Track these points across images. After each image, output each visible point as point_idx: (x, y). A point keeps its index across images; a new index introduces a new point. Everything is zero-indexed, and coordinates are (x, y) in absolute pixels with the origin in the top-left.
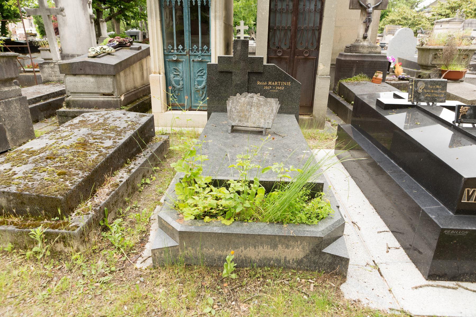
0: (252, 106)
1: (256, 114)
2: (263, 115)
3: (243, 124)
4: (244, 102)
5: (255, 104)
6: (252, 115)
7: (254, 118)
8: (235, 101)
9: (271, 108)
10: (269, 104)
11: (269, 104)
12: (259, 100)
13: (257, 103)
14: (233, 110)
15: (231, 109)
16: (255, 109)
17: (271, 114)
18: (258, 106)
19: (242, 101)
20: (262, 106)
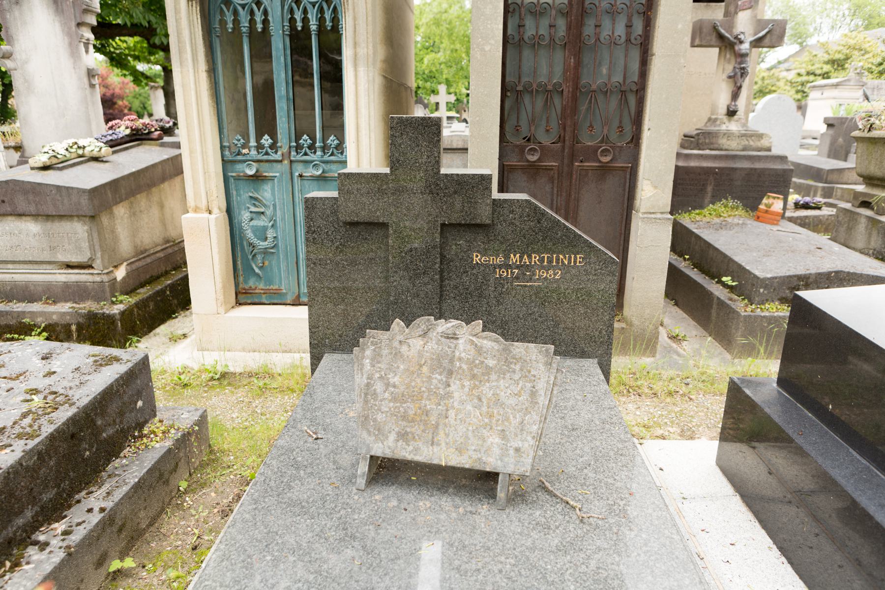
0: (450, 373)
1: (469, 407)
2: (497, 417)
3: (417, 450)
4: (420, 354)
5: (465, 367)
6: (452, 413)
7: (462, 429)
8: (385, 352)
9: (529, 385)
10: (518, 367)
11: (518, 367)
12: (479, 350)
13: (471, 363)
14: (379, 387)
15: (368, 385)
16: (463, 386)
17: (527, 412)
18: (474, 377)
19: (413, 352)
20: (493, 377)
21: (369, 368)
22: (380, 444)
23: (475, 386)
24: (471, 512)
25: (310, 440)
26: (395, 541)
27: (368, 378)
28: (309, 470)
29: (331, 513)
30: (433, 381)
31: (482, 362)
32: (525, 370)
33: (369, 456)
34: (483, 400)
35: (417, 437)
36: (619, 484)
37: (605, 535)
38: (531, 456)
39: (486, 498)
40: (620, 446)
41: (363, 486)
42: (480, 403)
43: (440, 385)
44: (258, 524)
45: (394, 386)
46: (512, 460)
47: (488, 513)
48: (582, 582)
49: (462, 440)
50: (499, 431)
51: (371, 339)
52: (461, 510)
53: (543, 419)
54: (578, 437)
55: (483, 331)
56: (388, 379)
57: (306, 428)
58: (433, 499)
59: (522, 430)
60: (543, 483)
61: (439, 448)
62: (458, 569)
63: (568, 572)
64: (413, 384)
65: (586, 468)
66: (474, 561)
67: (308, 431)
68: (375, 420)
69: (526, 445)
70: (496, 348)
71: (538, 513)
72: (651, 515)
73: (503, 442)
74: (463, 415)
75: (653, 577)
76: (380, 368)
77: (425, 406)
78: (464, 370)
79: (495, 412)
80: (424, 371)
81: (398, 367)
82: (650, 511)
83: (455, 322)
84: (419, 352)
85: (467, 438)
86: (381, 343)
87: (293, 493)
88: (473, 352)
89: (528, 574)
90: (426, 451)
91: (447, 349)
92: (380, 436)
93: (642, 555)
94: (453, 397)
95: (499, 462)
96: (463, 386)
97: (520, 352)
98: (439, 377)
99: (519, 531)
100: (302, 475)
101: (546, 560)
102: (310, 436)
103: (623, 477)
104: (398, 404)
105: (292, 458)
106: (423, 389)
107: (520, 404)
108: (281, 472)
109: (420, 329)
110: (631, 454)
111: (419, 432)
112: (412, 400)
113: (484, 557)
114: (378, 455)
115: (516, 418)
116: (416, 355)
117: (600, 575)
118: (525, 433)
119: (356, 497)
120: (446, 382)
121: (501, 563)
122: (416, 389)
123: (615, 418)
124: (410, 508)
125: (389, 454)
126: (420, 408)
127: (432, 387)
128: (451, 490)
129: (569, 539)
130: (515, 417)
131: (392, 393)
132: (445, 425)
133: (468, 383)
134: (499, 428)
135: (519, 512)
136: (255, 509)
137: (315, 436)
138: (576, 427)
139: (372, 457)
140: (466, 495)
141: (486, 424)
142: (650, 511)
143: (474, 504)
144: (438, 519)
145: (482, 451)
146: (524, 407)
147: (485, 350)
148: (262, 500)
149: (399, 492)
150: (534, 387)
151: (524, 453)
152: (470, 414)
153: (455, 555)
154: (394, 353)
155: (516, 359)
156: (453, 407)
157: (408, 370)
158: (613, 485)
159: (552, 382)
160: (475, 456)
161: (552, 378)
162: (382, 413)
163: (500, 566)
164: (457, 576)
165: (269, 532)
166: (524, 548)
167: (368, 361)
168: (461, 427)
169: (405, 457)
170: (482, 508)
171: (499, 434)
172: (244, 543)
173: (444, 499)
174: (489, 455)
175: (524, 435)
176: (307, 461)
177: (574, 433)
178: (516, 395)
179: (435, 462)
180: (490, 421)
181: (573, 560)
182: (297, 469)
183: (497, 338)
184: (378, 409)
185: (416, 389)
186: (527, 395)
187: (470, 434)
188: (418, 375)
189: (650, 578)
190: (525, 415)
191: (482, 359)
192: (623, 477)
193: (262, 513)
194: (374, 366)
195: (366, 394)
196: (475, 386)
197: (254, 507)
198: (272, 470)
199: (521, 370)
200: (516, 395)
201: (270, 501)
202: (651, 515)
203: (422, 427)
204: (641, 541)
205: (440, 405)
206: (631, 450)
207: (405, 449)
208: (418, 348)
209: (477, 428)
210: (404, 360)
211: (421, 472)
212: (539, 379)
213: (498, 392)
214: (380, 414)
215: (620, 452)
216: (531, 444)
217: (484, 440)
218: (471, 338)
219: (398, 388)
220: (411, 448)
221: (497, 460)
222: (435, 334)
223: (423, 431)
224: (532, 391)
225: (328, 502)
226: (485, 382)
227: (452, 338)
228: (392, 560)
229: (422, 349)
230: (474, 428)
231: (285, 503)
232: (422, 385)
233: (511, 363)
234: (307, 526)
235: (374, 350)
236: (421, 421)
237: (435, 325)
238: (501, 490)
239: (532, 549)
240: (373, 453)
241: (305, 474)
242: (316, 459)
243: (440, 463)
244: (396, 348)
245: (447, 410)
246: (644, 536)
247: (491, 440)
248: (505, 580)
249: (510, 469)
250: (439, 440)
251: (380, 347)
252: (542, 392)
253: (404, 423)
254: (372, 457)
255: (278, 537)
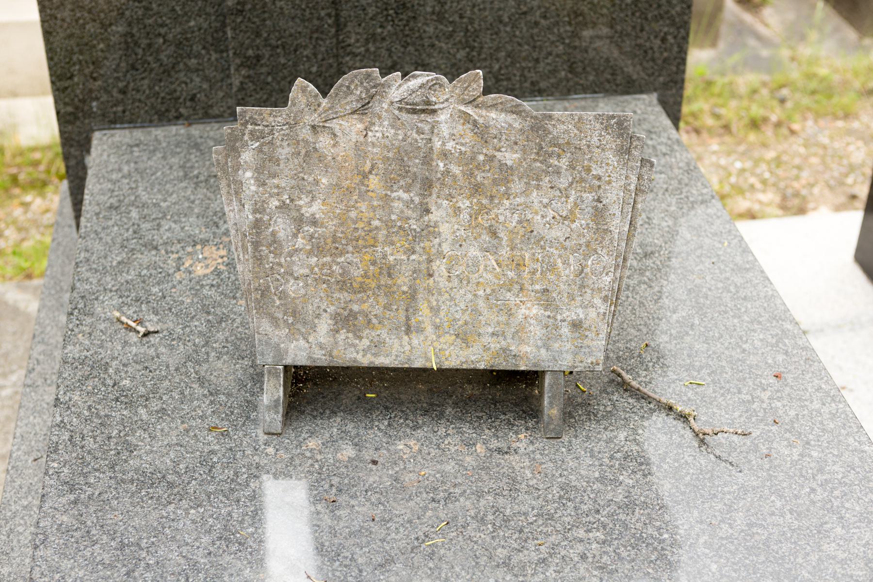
0: (427, 185)
1: (474, 252)
2: (530, 265)
3: (377, 345)
4: (359, 149)
5: (456, 170)
6: (440, 267)
7: (463, 296)
8: (284, 151)
9: (589, 197)
10: (564, 163)
11: (564, 163)
12: (482, 132)
13: (468, 161)
14: (281, 227)
15: (257, 225)
16: (457, 211)
17: (589, 250)
18: (477, 189)
19: (344, 149)
20: (517, 186)
21: (253, 188)
22: (302, 342)
23: (482, 207)
24: (499, 451)
25: (133, 338)
26: (375, 528)
27: (255, 211)
28: (155, 405)
29: (232, 490)
30: (396, 204)
31: (492, 158)
32: (579, 168)
33: (281, 367)
34: (501, 235)
35: (374, 321)
36: (752, 360)
37: (750, 461)
38: (603, 336)
39: (520, 418)
40: (738, 280)
41: (278, 427)
42: (495, 242)
43: (409, 213)
44: (94, 532)
45: (314, 222)
46: (568, 346)
47: (531, 448)
48: (728, 555)
49: (466, 317)
50: (536, 292)
51: (250, 127)
52: (480, 448)
53: (620, 260)
54: (659, 270)
55: (486, 91)
56: (298, 209)
57: (117, 314)
58: (420, 433)
59: (582, 286)
60: (619, 375)
61: (422, 338)
62: (506, 564)
63: (701, 541)
64: (353, 214)
65: (687, 334)
66: (531, 544)
67: (124, 319)
68: (283, 295)
69: (593, 314)
70: (517, 125)
71: (622, 435)
72: (819, 412)
73: (548, 313)
74: (463, 268)
75: (843, 527)
76: (278, 187)
77: (385, 257)
78: (454, 177)
79: (527, 255)
80: (372, 187)
81: (317, 182)
82: (816, 405)
83: (421, 78)
84: (357, 146)
85: (476, 312)
86: (271, 133)
87: (140, 457)
88: (469, 138)
89: (633, 556)
90: (396, 345)
91: (415, 135)
92: (299, 326)
93: (819, 490)
94: (439, 234)
95: (543, 351)
96: (457, 211)
97: (566, 132)
98: (405, 196)
99: (597, 475)
100: (144, 417)
101: (658, 524)
102: (129, 328)
103: (758, 344)
104: (328, 259)
105: (110, 382)
106: (376, 223)
107: (575, 236)
108: (98, 416)
109: (353, 98)
110: (762, 294)
111: (378, 310)
112: (355, 247)
113: (547, 535)
114: (299, 364)
115: (569, 265)
116: (351, 153)
117: (757, 537)
118: (589, 291)
119: (271, 450)
120: (421, 204)
121: (581, 541)
122: (360, 225)
123: (718, 222)
124: (383, 456)
125: (321, 358)
126: (374, 263)
127: (393, 217)
128: (449, 411)
129: (688, 478)
130: (566, 263)
131: (312, 237)
132: (430, 291)
133: (468, 203)
134: (538, 287)
135: (588, 438)
136: (75, 502)
137: (142, 330)
138: (649, 249)
139: (286, 368)
140: (480, 418)
141: (512, 282)
142: (816, 405)
143: (500, 434)
144: (444, 474)
145: (509, 335)
146: (583, 241)
147: (494, 132)
148: (81, 480)
149: (350, 427)
150: (599, 200)
151: (589, 329)
152: (476, 264)
153: (493, 537)
154: (303, 152)
155: (559, 146)
156: (441, 255)
157: (338, 186)
158: (743, 361)
159: (633, 187)
160: (495, 346)
161: (634, 179)
162: (297, 279)
163: (580, 548)
164: (508, 578)
165: (122, 546)
166: (613, 507)
167: (249, 174)
168: (462, 292)
169: (355, 361)
170: (519, 440)
171: (537, 299)
172: (81, 574)
173: (442, 431)
174: (522, 341)
175: (588, 296)
176: (144, 385)
177: (649, 262)
178: (565, 218)
179: (418, 364)
180: (519, 275)
181: (704, 518)
182: (129, 404)
183: (518, 106)
184: (286, 273)
185: (360, 225)
186: (587, 216)
187: (481, 304)
188: (360, 195)
189: (839, 530)
190: (586, 257)
191: (491, 152)
192: (758, 344)
193: (92, 509)
194: (264, 184)
195: (256, 245)
196: (482, 207)
197: (72, 497)
198: (79, 415)
199: (572, 167)
200: (565, 218)
201: (100, 481)
202: (819, 412)
203: (383, 300)
204: (813, 465)
205: (414, 252)
206: (760, 287)
207: (354, 346)
208: (354, 137)
209: (493, 291)
210: (326, 166)
211: (381, 380)
212: (609, 183)
213: (529, 216)
214: (292, 281)
215: (742, 294)
216: (602, 311)
217: (510, 314)
218: (463, 108)
219: (322, 225)
220: (366, 342)
221: (538, 348)
222: (385, 106)
223: (387, 307)
224: (596, 208)
225: (219, 466)
226: (501, 199)
227: (423, 111)
228: (381, 566)
229: (362, 139)
230: (488, 291)
231: (132, 481)
232: (372, 214)
233: (550, 156)
234: (194, 522)
235: (260, 150)
236: (379, 287)
237: (383, 85)
238: (551, 403)
239: (629, 506)
240: (289, 361)
241: (150, 413)
242: (161, 379)
243: (428, 365)
244: (306, 142)
245: (430, 261)
246: (815, 454)
247: (523, 311)
248: (595, 573)
249: (565, 363)
250: (420, 322)
251: (271, 143)
252: (615, 210)
253: (345, 296)
254: (286, 368)
255: (144, 554)
